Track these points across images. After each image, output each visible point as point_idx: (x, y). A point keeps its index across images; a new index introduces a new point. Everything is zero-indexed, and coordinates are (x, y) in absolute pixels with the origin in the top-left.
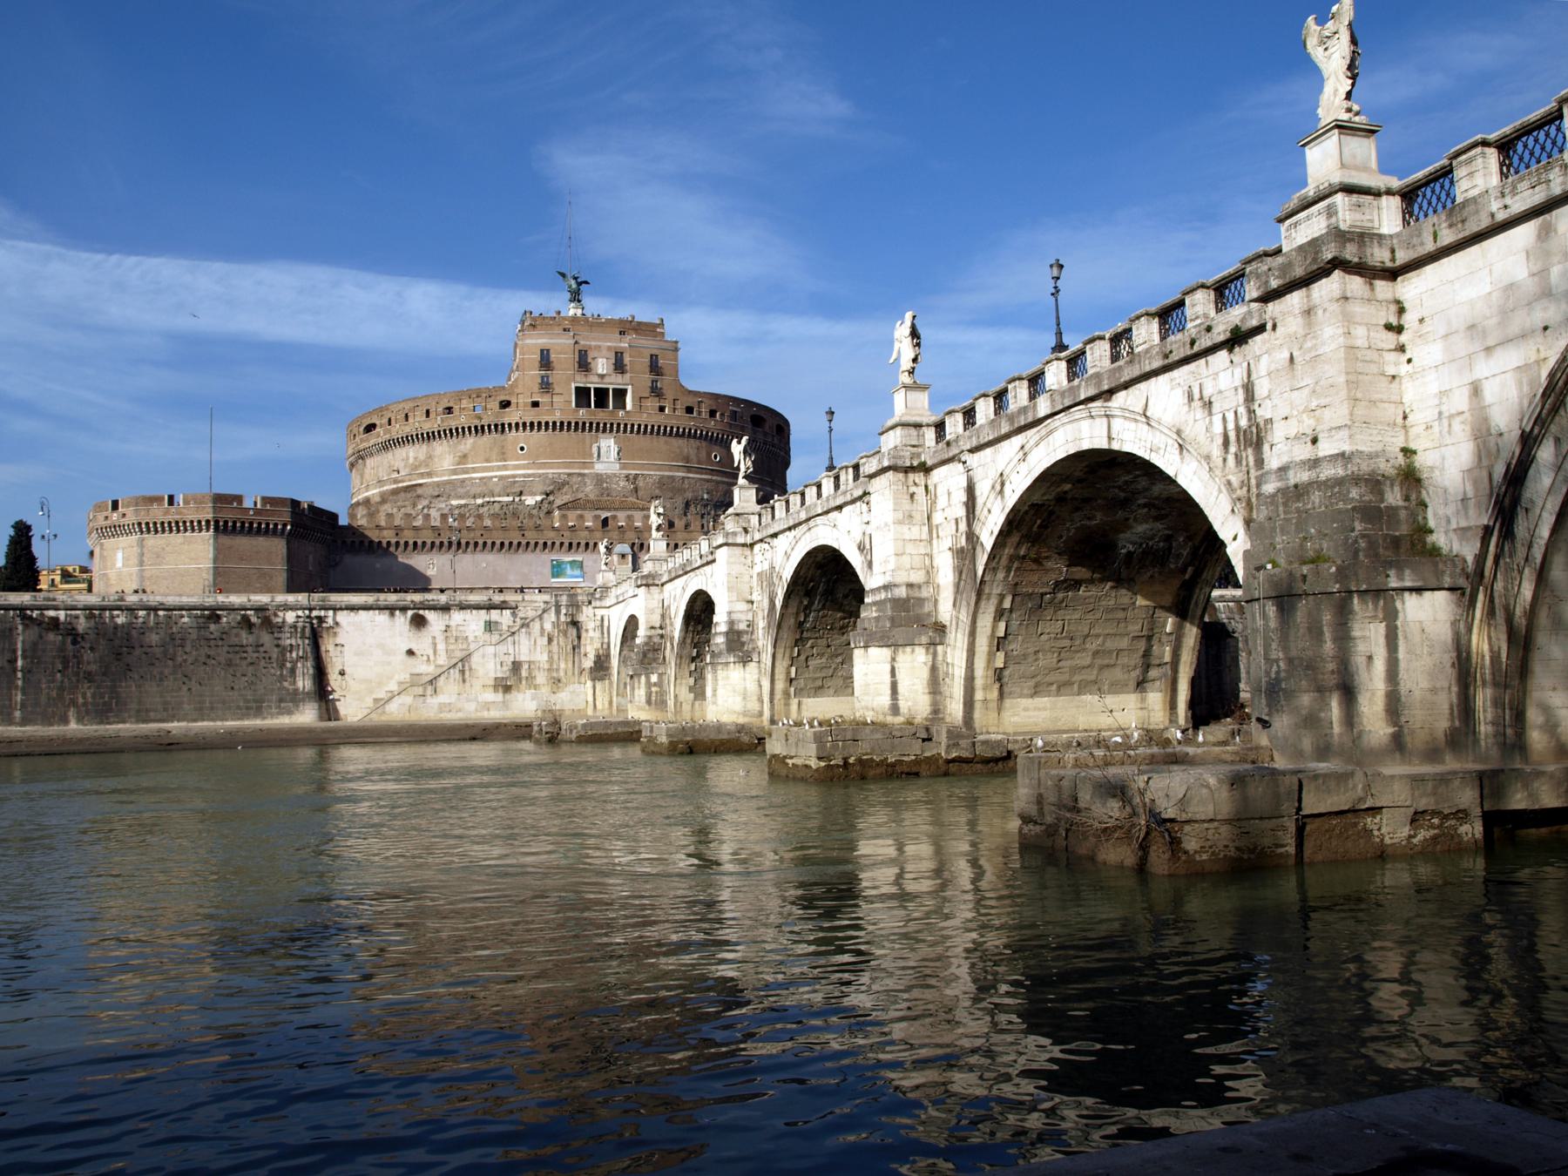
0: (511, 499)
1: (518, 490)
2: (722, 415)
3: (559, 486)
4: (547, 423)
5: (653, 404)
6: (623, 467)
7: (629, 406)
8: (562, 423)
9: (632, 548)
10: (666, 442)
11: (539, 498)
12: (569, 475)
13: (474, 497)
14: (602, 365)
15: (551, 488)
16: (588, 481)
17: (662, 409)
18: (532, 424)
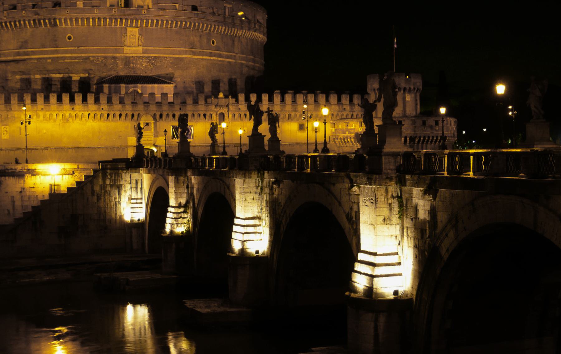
0: (61, 76)
4: (88, 19)
11: (82, 75)
12: (105, 58)
16: (119, 62)
18: (77, 20)
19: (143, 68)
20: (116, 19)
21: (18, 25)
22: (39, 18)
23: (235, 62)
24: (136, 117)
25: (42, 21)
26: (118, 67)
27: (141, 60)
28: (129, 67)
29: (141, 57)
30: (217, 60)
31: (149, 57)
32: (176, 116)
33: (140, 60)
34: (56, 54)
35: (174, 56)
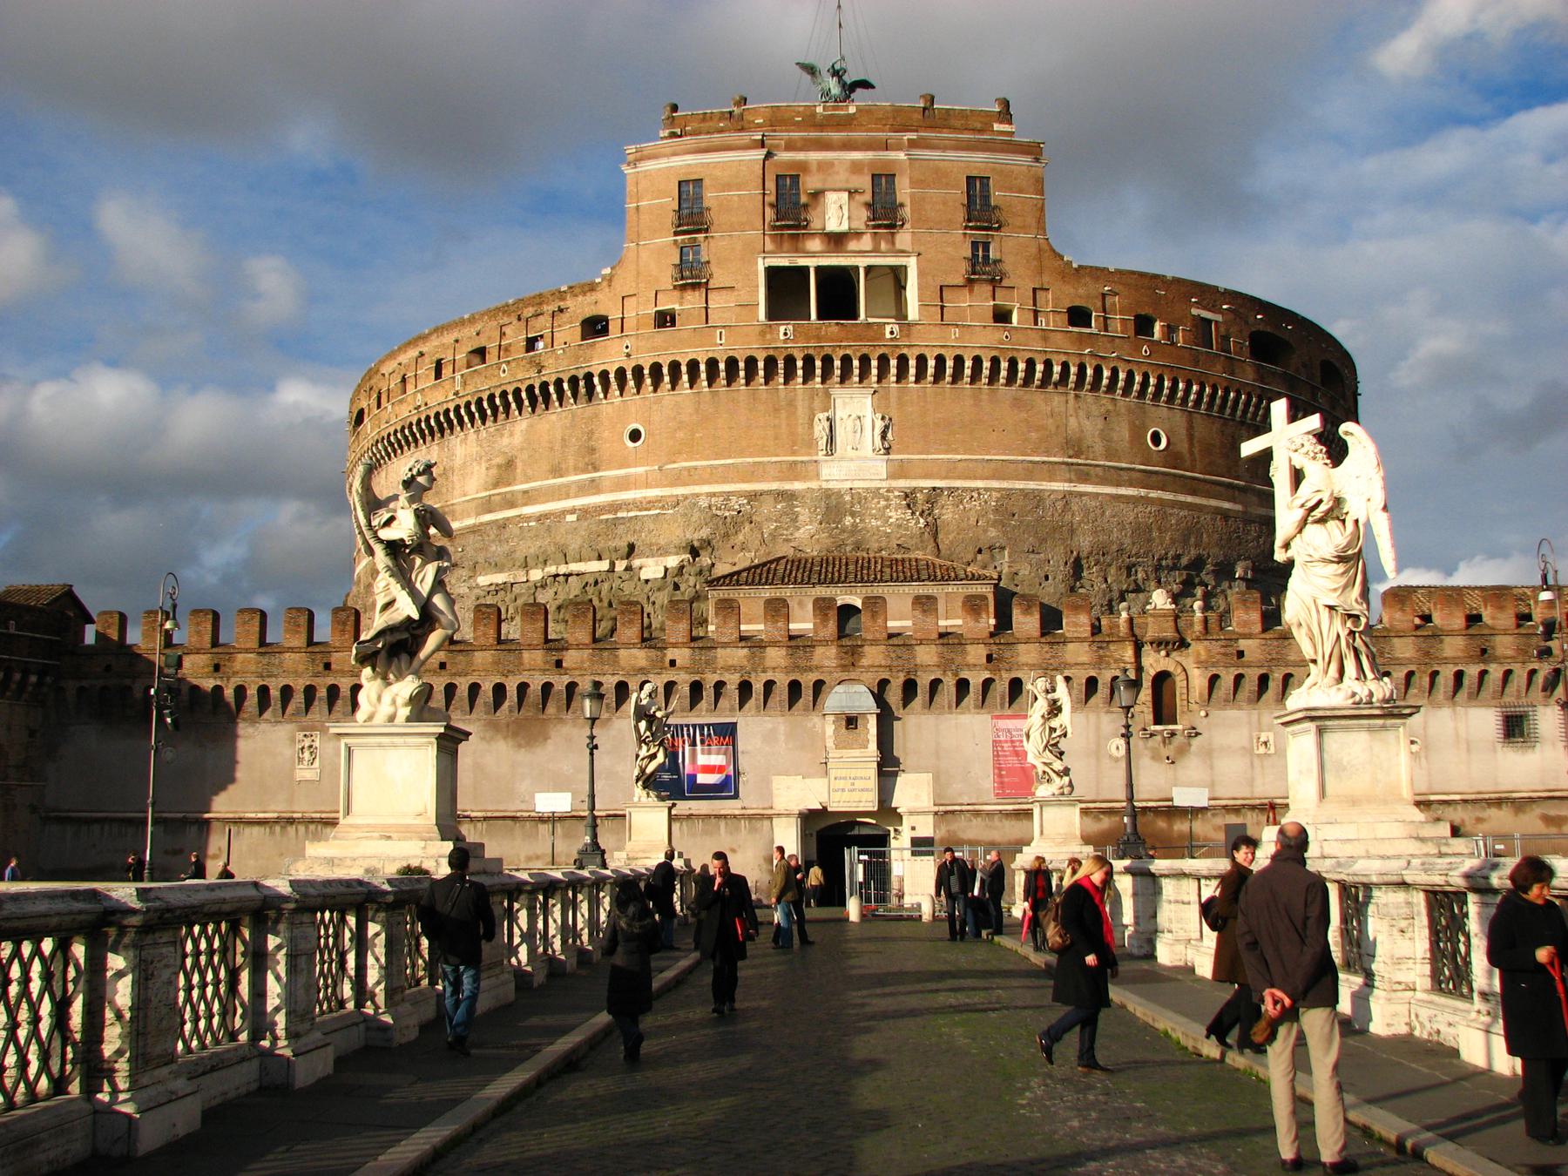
1: (622, 544)
2: (1170, 330)
3: (729, 525)
5: (980, 302)
6: (898, 472)
7: (913, 312)
8: (732, 363)
9: (879, 696)
10: (1017, 403)
11: (673, 562)
12: (753, 497)
13: (526, 566)
14: (836, 213)
15: (704, 533)
16: (803, 513)
17: (1002, 316)
19: (889, 531)
20: (790, 361)
21: (489, 412)
22: (544, 379)
23: (1243, 512)
24: (807, 693)
25: (552, 389)
26: (798, 529)
27: (883, 503)
28: (837, 527)
29: (881, 491)
30: (1174, 504)
31: (914, 491)
32: (971, 689)
33: (879, 503)
34: (595, 494)
35: (1005, 485)
